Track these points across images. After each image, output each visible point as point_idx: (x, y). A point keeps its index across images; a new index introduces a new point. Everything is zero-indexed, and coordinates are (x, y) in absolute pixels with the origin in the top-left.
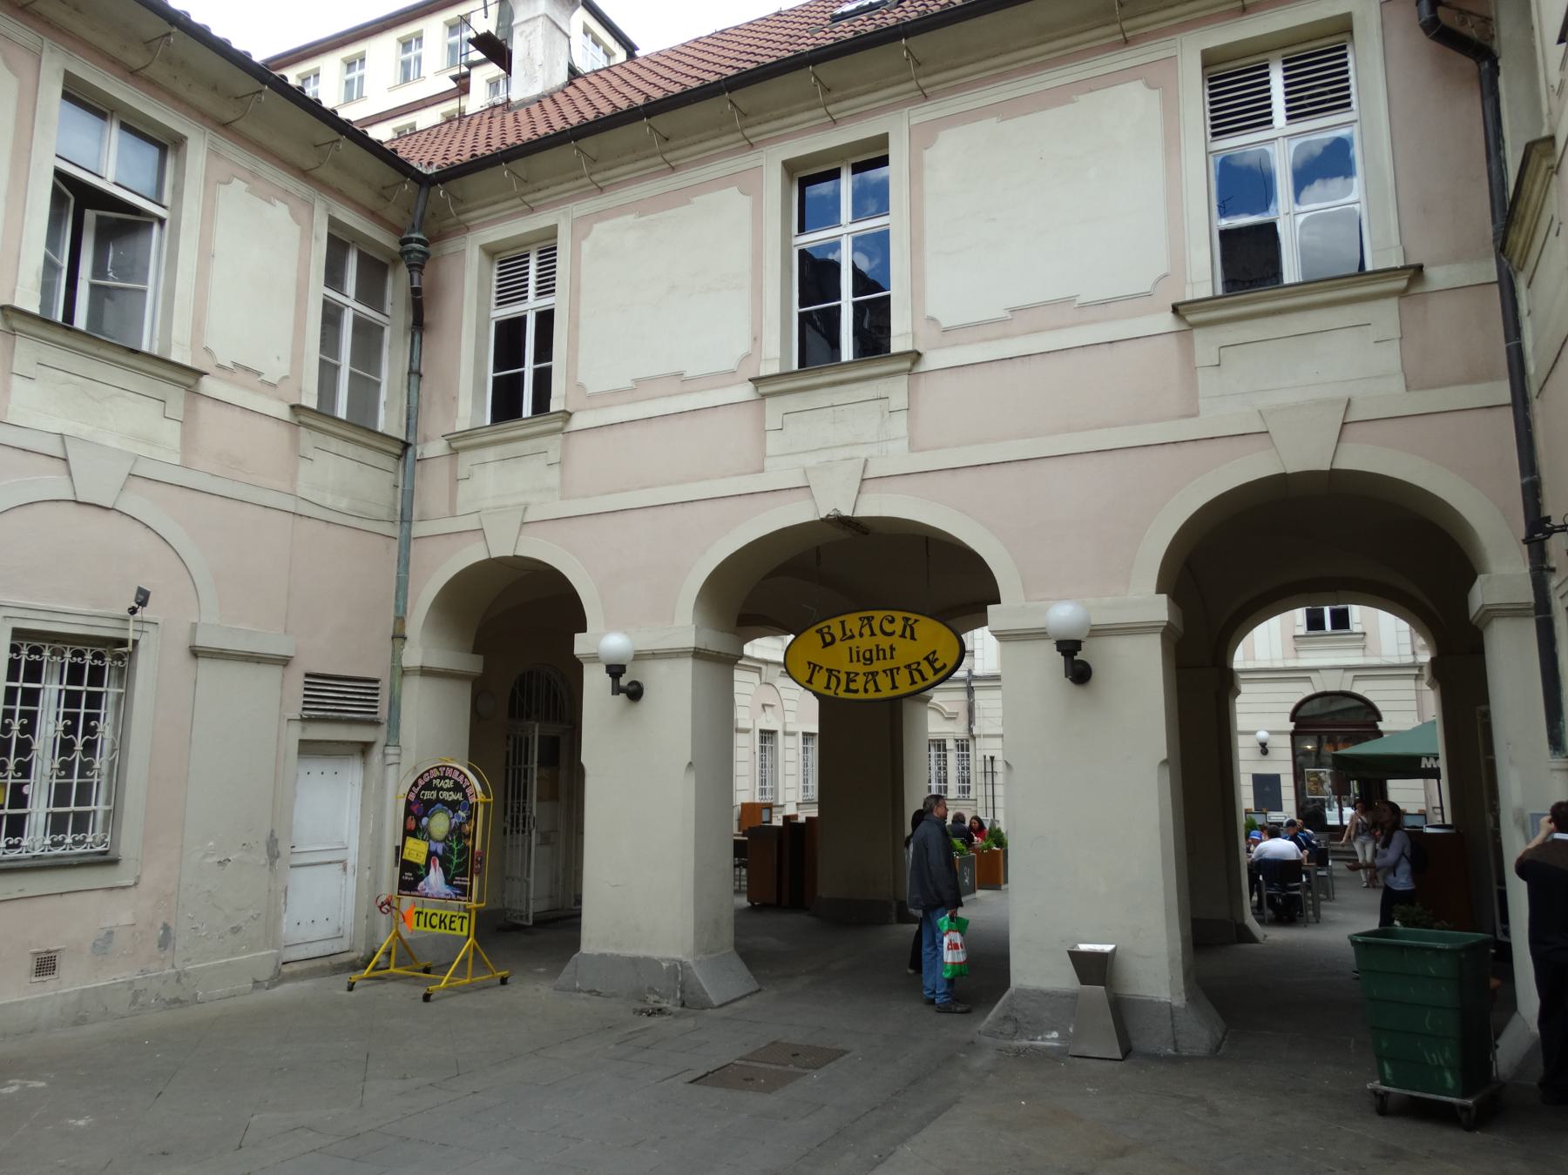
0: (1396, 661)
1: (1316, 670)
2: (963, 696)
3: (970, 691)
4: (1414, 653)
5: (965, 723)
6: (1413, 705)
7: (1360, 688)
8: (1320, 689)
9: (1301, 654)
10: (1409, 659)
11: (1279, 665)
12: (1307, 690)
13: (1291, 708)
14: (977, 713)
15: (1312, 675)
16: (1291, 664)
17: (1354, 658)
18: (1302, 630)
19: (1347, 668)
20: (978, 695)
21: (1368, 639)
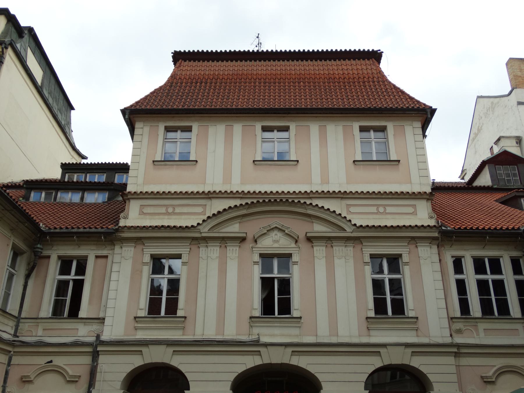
0: (440, 341)
1: (384, 345)
2: (87, 360)
3: (95, 355)
4: (451, 335)
5: (86, 386)
6: (454, 378)
7: (416, 362)
8: (387, 362)
9: (372, 333)
10: (448, 340)
11: (356, 340)
12: (376, 363)
13: (365, 377)
14: (98, 376)
15: (382, 350)
16: (365, 340)
17: (410, 338)
18: (372, 314)
19: (407, 345)
20: (102, 359)
21: (420, 324)
